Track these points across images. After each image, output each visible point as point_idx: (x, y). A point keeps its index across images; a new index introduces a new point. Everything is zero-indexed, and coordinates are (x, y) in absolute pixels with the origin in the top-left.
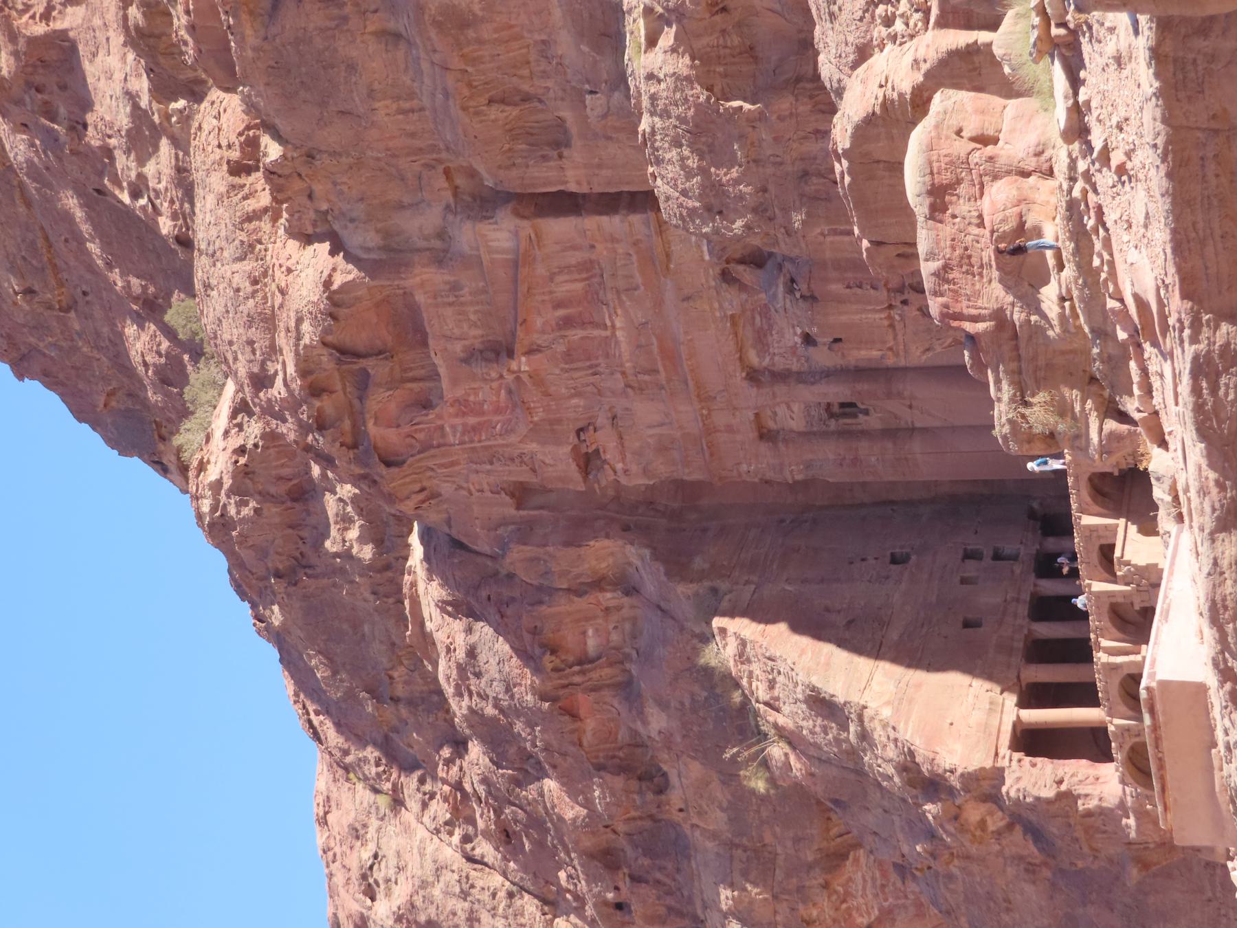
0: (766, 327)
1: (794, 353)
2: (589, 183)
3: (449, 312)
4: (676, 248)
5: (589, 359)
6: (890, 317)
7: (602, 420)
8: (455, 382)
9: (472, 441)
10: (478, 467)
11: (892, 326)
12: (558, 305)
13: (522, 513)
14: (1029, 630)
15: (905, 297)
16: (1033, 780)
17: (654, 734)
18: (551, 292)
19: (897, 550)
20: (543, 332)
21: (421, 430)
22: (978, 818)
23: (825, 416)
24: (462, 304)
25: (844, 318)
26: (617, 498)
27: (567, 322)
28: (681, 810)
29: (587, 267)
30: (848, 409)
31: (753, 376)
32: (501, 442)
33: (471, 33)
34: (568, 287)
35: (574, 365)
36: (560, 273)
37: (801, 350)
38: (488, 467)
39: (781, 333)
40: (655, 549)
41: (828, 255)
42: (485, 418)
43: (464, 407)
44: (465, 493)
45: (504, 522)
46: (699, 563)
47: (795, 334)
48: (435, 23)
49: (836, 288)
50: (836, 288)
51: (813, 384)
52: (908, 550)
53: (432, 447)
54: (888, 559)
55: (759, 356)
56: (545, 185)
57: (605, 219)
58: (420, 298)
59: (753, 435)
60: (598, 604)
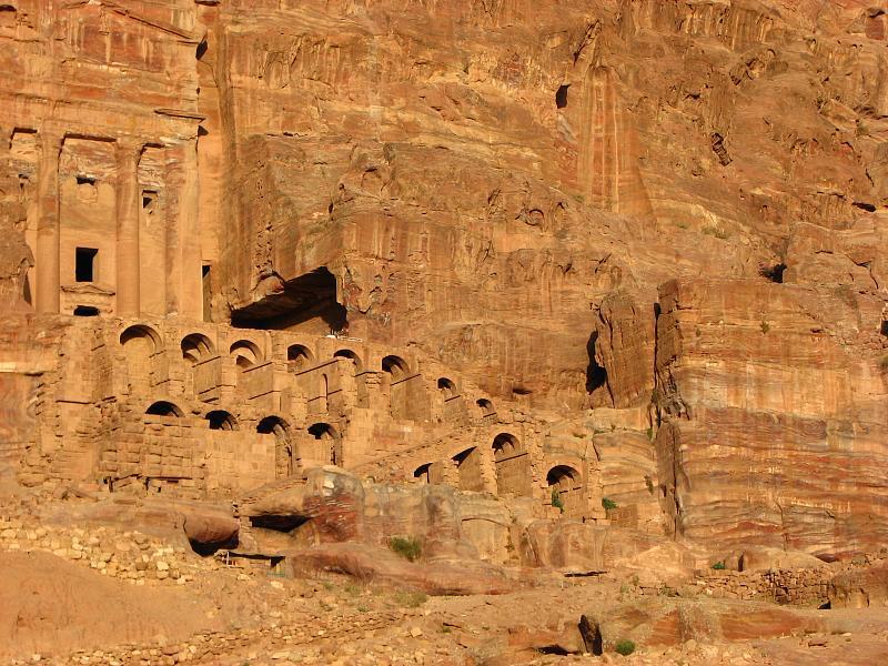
4: (172, 122)
5: (85, 42)
12: (132, 39)
18: (142, 37)
27: (117, 39)
29: (157, 64)
33: (348, 56)
34: (145, 48)
36: (155, 48)
39: (89, 165)
48: (357, 39)
49: (393, 232)
56: (239, 61)
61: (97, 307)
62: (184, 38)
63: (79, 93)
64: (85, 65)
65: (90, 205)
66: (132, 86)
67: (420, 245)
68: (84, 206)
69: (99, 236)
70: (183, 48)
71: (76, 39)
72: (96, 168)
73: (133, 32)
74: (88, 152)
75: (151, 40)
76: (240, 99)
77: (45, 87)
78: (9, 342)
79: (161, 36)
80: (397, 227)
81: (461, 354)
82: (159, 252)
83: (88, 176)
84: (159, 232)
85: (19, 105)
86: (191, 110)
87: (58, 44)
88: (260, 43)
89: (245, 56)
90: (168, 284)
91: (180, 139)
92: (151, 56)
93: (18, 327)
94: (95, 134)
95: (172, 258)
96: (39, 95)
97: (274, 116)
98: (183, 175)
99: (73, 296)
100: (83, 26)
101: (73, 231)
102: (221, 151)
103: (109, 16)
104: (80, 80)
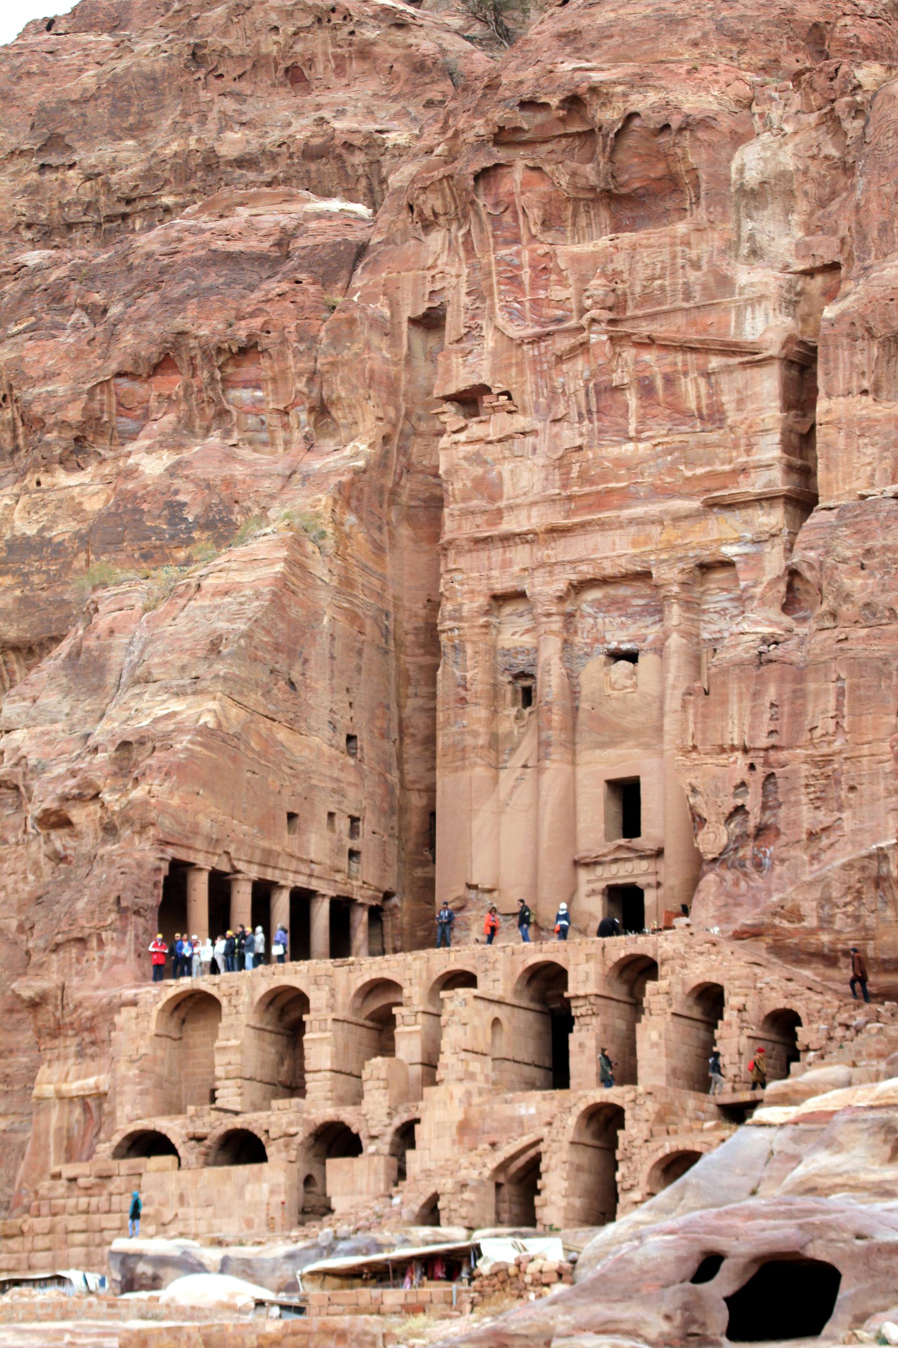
1: (596, 640)
2: (827, 423)
3: (666, 256)
5: (598, 412)
6: (733, 748)
7: (520, 422)
8: (576, 259)
9: (499, 274)
10: (464, 278)
11: (723, 750)
12: (670, 381)
13: (405, 326)
14: (282, 887)
15: (759, 768)
16: (142, 884)
17: (131, 461)
18: (686, 374)
20: (636, 362)
21: (516, 218)
22: (74, 820)
24: (673, 273)
25: (734, 698)
26: (416, 433)
27: (646, 389)
28: (39, 483)
29: (714, 416)
30: (527, 697)
32: (497, 306)
34: (692, 391)
35: (592, 395)
36: (710, 385)
37: (601, 648)
38: (464, 290)
40: (364, 472)
41: (812, 686)
42: (527, 288)
43: (543, 269)
44: (430, 262)
45: (394, 305)
46: (351, 519)
47: (621, 642)
49: (771, 693)
50: (771, 693)
51: (561, 659)
53: (495, 229)
54: (351, 732)
56: (827, 374)
57: (777, 437)
58: (681, 228)
60: (294, 405)
62: (749, 356)
63: (590, 507)
64: (604, 452)
65: (624, 700)
66: (672, 470)
67: (832, 704)
68: (615, 704)
69: (638, 751)
70: (755, 372)
71: (584, 411)
72: (634, 629)
73: (668, 370)
77: (535, 512)
78: (93, 1043)
79: (715, 362)
80: (782, 680)
81: (880, 905)
85: (496, 554)
86: (769, 483)
87: (556, 428)
88: (860, 330)
89: (836, 359)
91: (754, 542)
92: (704, 402)
93: (93, 1018)
96: (517, 530)
97: (882, 459)
99: (599, 870)
100: (591, 385)
103: (629, 353)
104: (592, 483)
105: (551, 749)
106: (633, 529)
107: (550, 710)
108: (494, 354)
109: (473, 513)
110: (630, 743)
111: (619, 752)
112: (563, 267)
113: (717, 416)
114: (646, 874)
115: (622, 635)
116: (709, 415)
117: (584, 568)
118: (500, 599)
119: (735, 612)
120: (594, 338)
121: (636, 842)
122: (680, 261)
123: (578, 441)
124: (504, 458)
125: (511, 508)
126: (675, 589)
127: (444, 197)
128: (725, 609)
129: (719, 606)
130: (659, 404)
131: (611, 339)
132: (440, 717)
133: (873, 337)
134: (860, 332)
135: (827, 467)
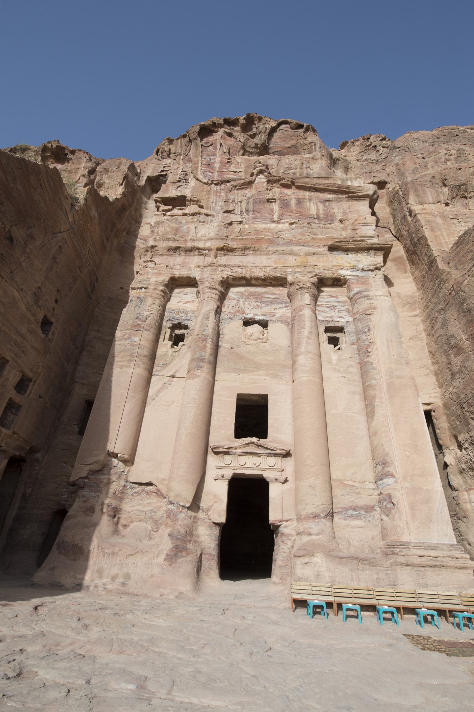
0: (264, 300)
1: (238, 312)
3: (298, 162)
12: (299, 202)
18: (310, 200)
19: (53, 328)
21: (215, 148)
23: (176, 322)
24: (301, 168)
29: (329, 218)
31: (227, 284)
46: (94, 213)
47: (257, 315)
52: (50, 336)
55: (237, 292)
56: (417, 196)
59: (177, 274)
61: (267, 475)
71: (244, 210)
72: (266, 309)
74: (258, 298)
75: (320, 202)
76: (429, 221)
82: (354, 393)
83: (257, 318)
84: (351, 370)
85: (179, 259)
87: (226, 214)
90: (372, 435)
91: (363, 270)
92: (321, 212)
94: (259, 273)
95: (374, 397)
98: (372, 302)
101: (234, 375)
102: (416, 289)
105: (202, 364)
106: (275, 256)
107: (205, 340)
108: (193, 187)
109: (168, 239)
110: (261, 372)
111: (251, 377)
112: (239, 161)
113: (330, 218)
114: (272, 468)
115: (258, 311)
116: (324, 218)
117: (240, 270)
118: (175, 283)
119: (342, 308)
120: (258, 180)
121: (262, 441)
122: (305, 166)
123: (241, 220)
124: (193, 222)
125: (193, 240)
126: (309, 285)
127: (176, 147)
128: (334, 306)
129: (330, 304)
130: (292, 212)
131: (268, 182)
132: (118, 333)
133: (445, 186)
134: (439, 181)
135: (432, 230)
